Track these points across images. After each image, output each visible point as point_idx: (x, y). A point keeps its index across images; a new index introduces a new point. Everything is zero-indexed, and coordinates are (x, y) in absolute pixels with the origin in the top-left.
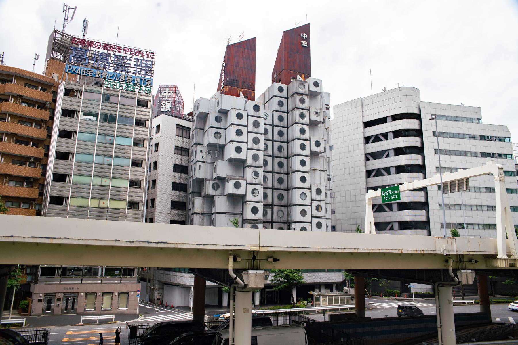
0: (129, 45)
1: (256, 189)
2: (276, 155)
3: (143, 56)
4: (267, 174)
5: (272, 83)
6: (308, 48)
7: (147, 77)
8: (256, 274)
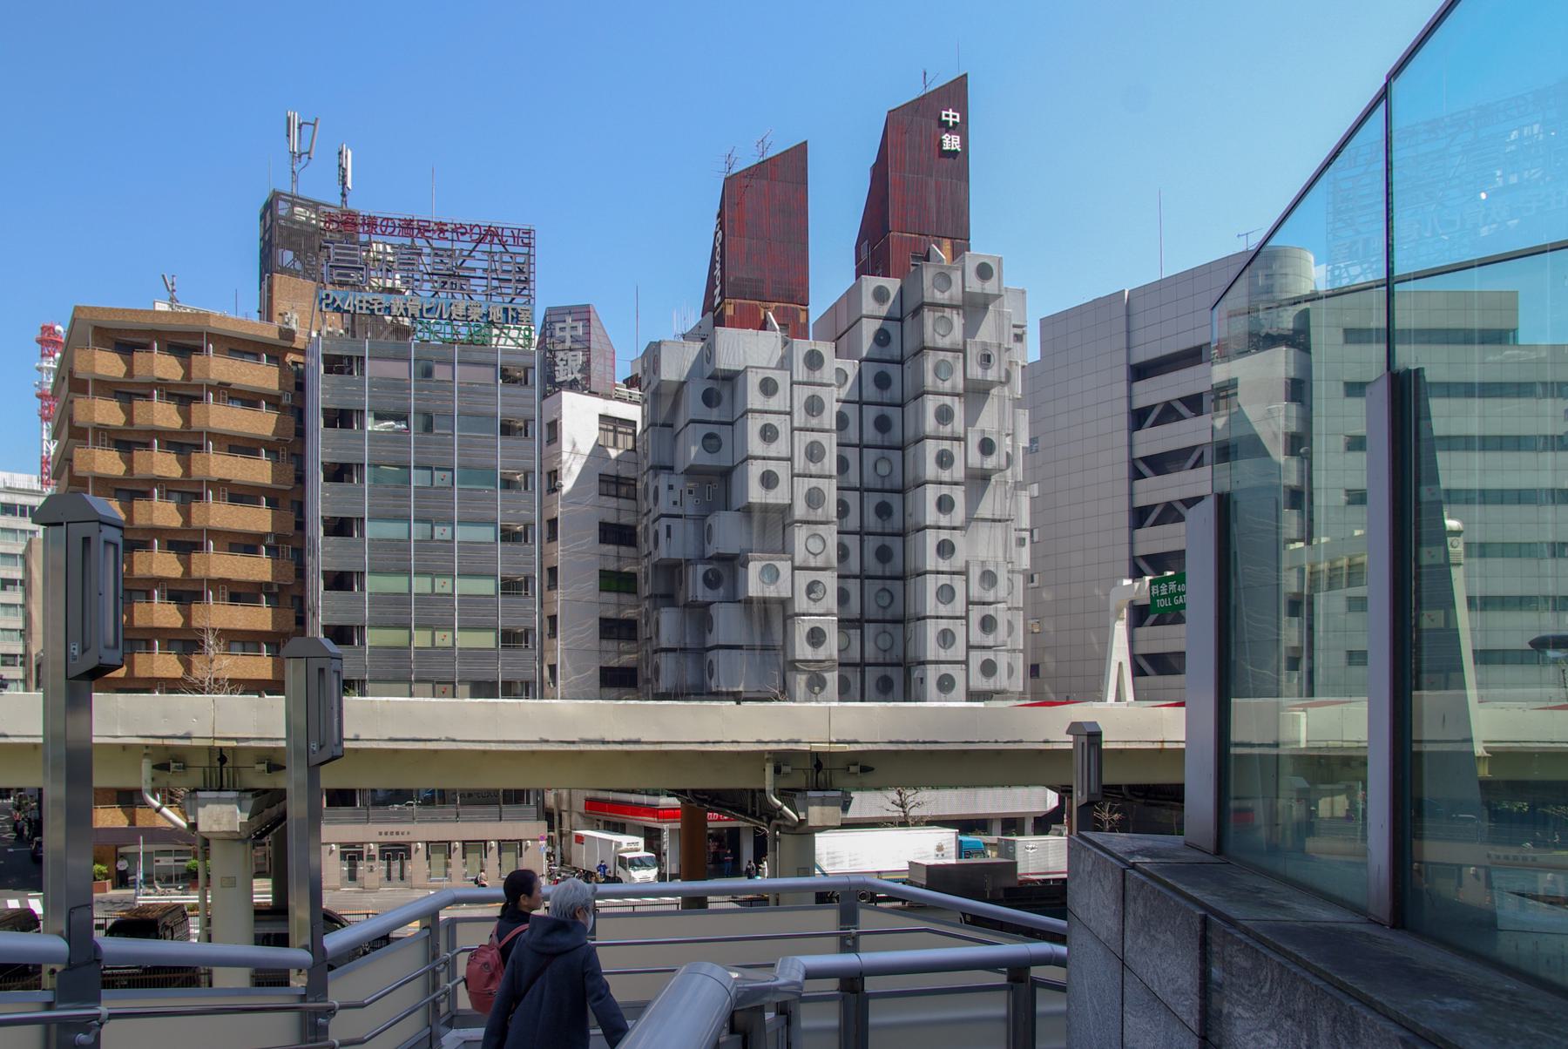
0: (467, 220)
1: (819, 582)
2: (871, 486)
4: (847, 539)
5: (858, 277)
6: (959, 159)
7: (519, 300)
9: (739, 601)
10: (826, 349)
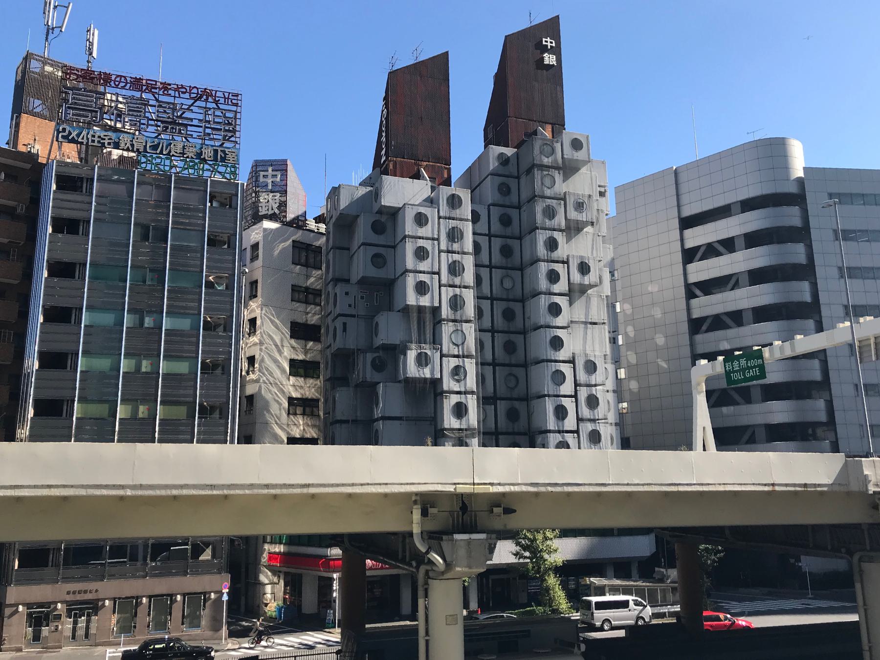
3: (216, 102)
5: (486, 146)
7: (227, 144)
8: (469, 542)
9: (400, 382)
10: (465, 195)
